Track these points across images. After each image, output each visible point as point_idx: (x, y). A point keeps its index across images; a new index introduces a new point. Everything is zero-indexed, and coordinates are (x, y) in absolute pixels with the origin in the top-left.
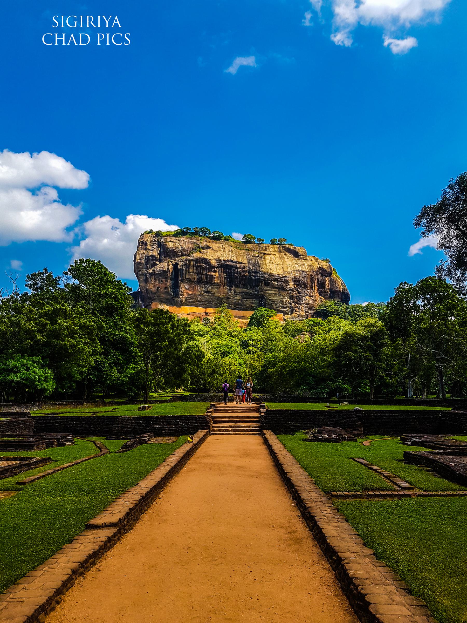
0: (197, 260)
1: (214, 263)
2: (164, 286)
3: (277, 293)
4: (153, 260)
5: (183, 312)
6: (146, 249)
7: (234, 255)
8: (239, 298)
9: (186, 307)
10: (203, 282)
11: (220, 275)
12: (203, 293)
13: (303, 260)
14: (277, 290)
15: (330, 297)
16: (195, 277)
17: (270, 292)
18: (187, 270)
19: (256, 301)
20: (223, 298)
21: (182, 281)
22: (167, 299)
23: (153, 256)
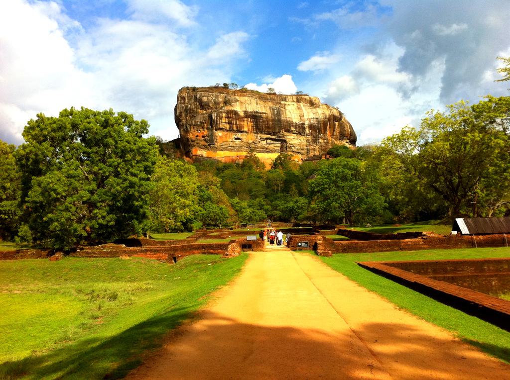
0: (228, 112)
1: (242, 114)
2: (202, 135)
3: (296, 137)
4: (190, 113)
5: (218, 156)
6: (184, 103)
8: (264, 142)
9: (221, 152)
10: (234, 131)
12: (234, 140)
13: (317, 109)
14: (295, 135)
15: (340, 140)
18: (220, 121)
19: (279, 144)
21: (216, 130)
22: (205, 146)
23: (190, 109)
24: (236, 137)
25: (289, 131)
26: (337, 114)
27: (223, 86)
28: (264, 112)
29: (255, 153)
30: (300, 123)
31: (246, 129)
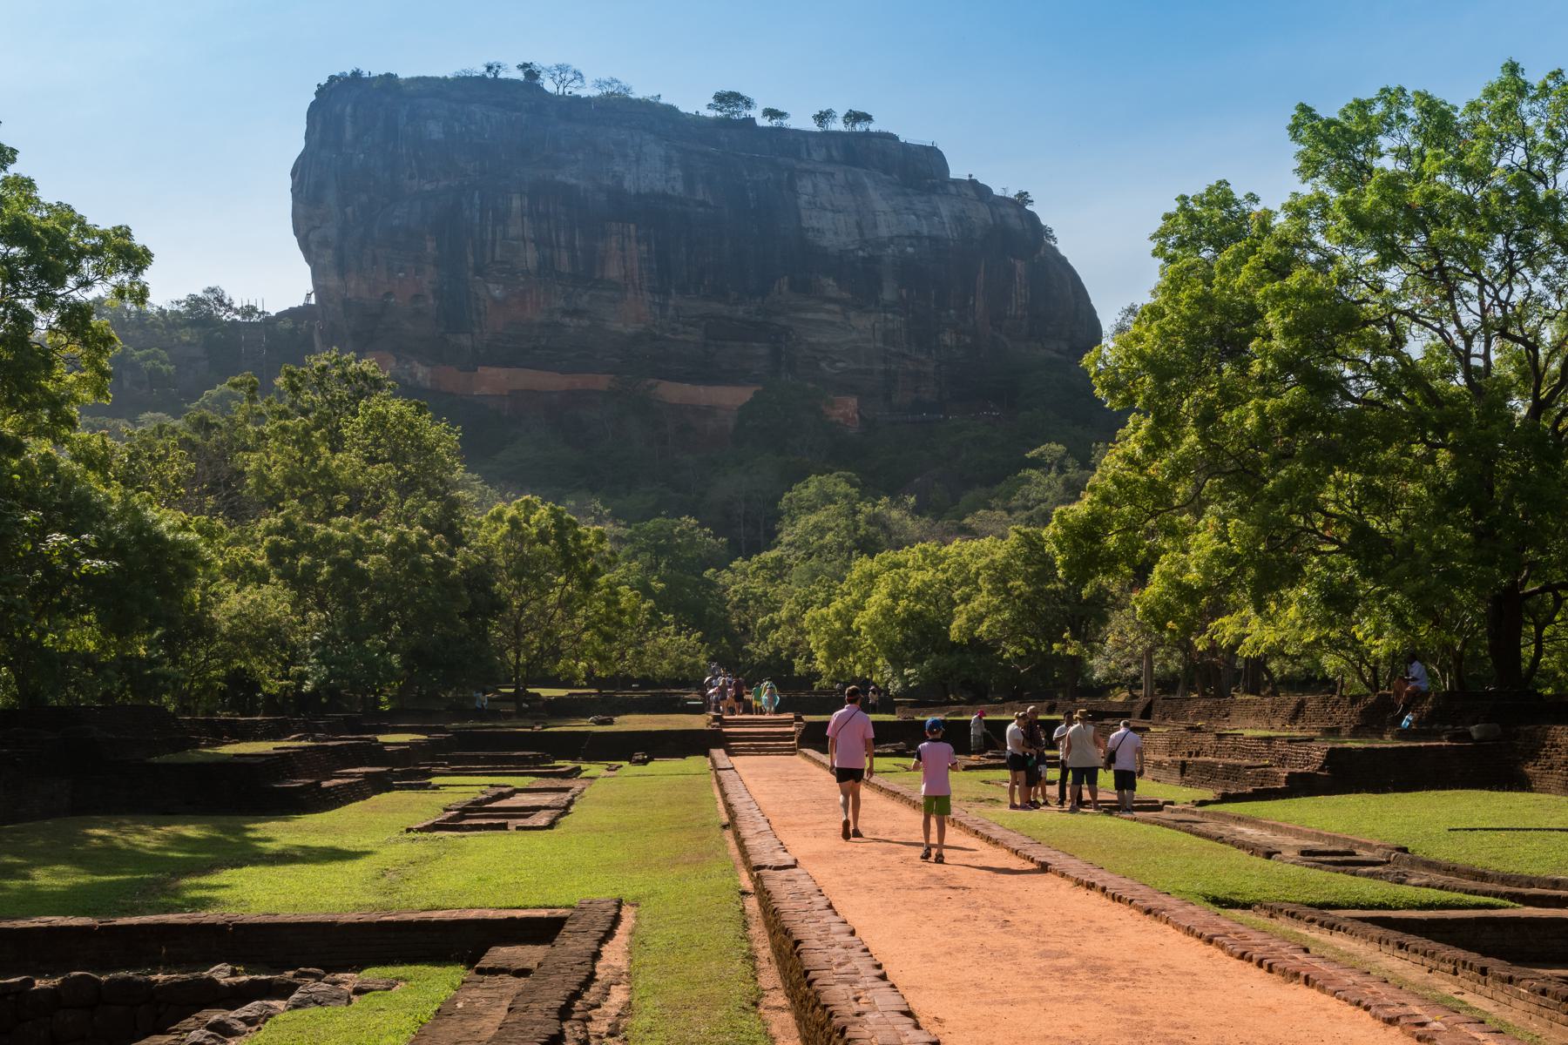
7: (676, 172)
9: (494, 370)
11: (623, 249)
14: (836, 308)
16: (530, 257)
17: (809, 316)
24: (561, 303)
26: (1014, 222)
27: (519, 75)
28: (700, 197)
29: (651, 381)
30: (861, 253)
31: (613, 271)
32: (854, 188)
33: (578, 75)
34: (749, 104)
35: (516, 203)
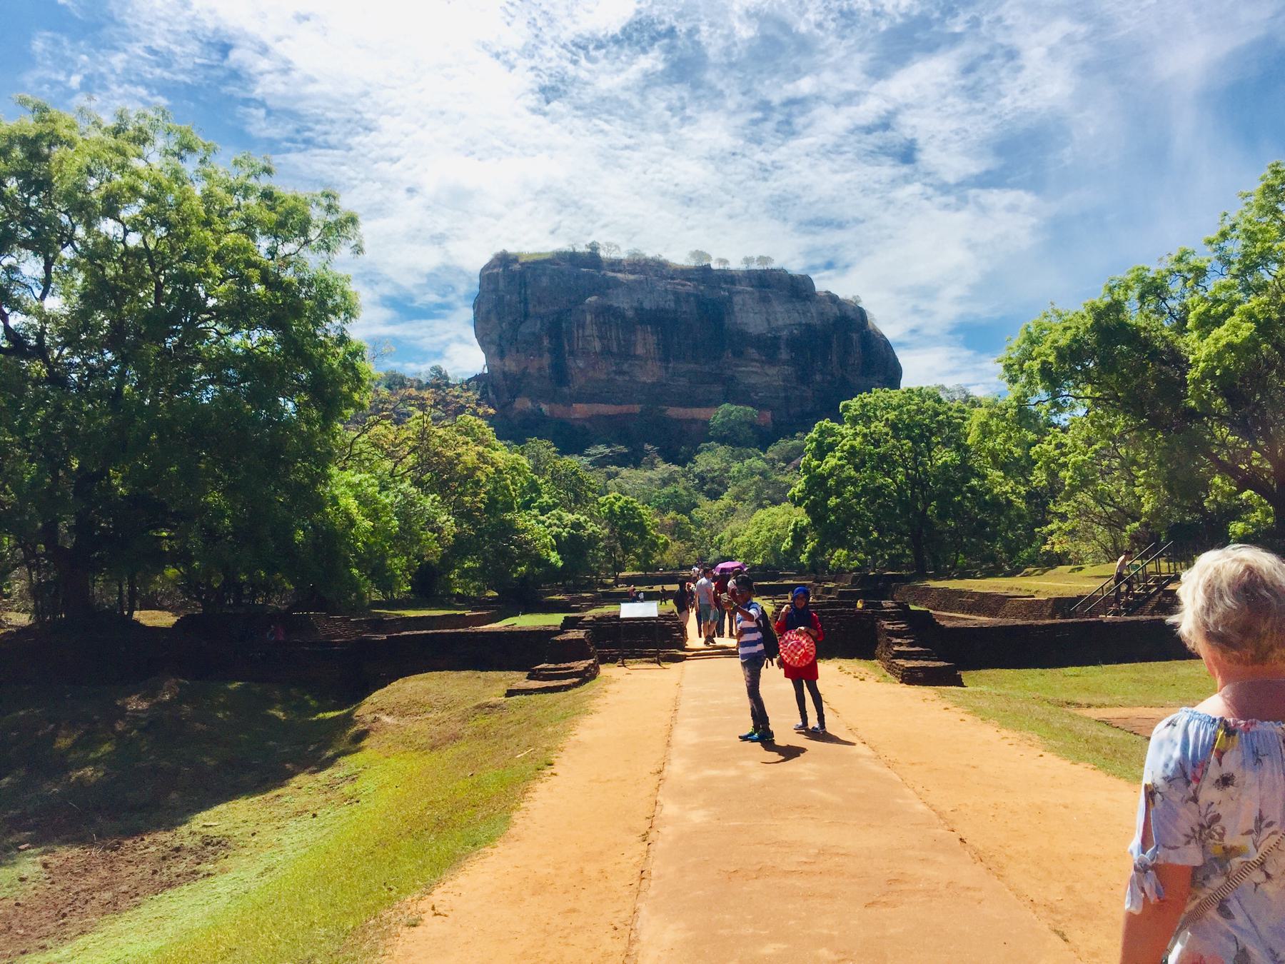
1: (630, 314)
5: (577, 416)
20: (653, 384)
21: (572, 353)
25: (739, 354)
26: (851, 314)
31: (640, 351)
32: (765, 300)
33: (617, 247)
34: (709, 257)
35: (589, 318)
